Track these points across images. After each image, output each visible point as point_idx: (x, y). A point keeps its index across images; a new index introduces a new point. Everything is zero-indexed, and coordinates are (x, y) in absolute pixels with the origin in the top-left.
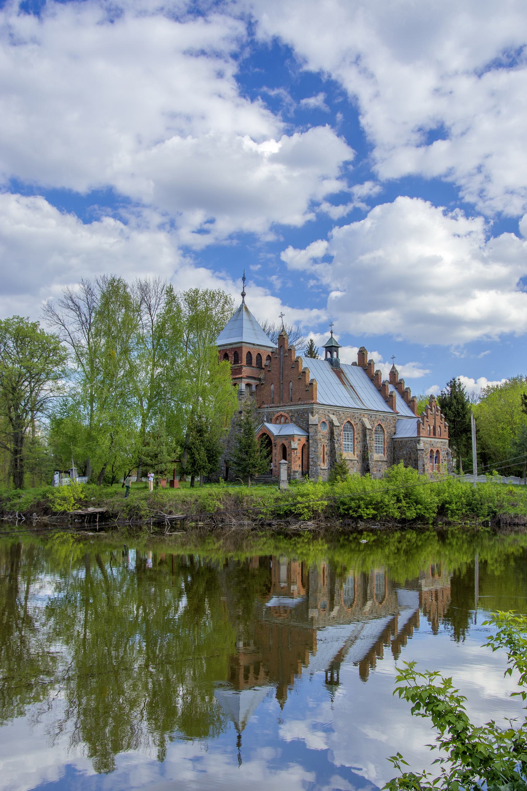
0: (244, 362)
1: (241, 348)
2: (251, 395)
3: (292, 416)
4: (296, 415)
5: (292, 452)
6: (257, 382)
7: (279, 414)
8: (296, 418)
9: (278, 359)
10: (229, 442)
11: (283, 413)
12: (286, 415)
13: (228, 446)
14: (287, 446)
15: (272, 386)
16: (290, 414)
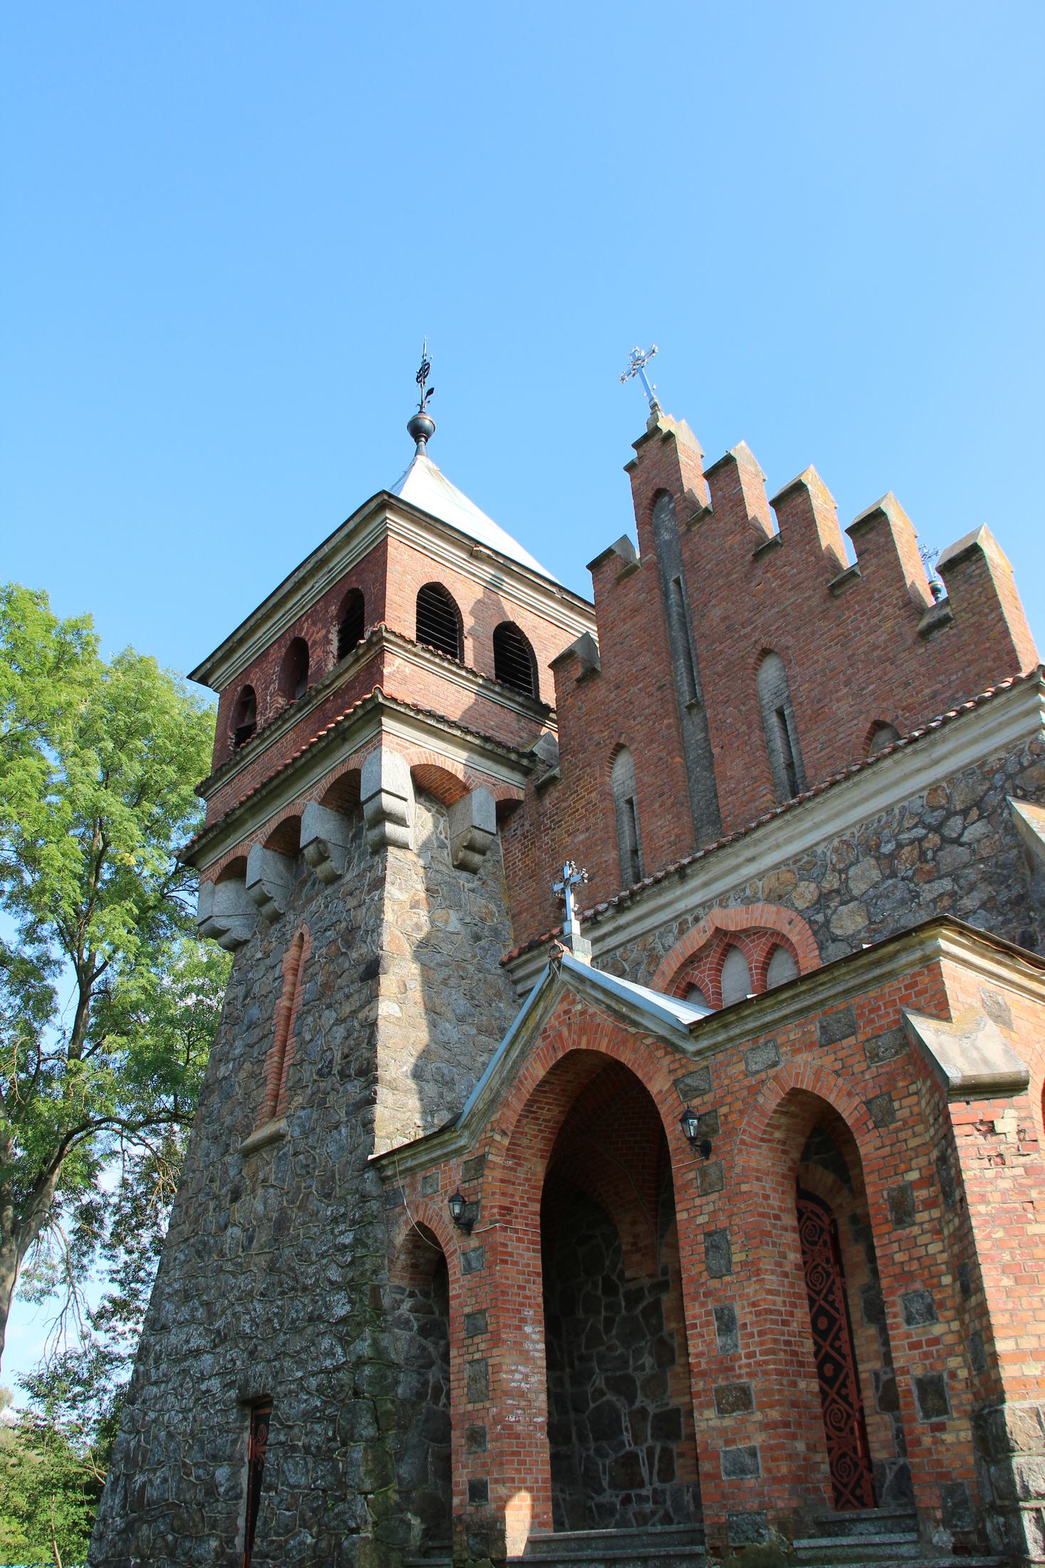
0: (401, 614)
1: (376, 560)
2: (462, 866)
3: (823, 900)
4: (865, 875)
5: (967, 1142)
6: (513, 784)
7: (697, 937)
8: (869, 903)
9: (642, 574)
10: (281, 1224)
11: (734, 918)
12: (766, 915)
13: (272, 1269)
14: (848, 1109)
15: (622, 773)
16: (806, 892)
